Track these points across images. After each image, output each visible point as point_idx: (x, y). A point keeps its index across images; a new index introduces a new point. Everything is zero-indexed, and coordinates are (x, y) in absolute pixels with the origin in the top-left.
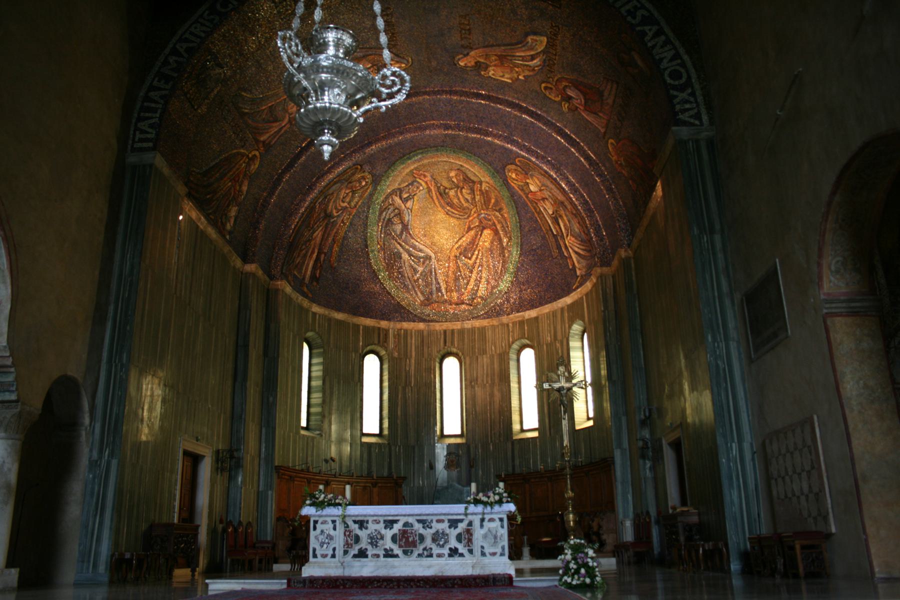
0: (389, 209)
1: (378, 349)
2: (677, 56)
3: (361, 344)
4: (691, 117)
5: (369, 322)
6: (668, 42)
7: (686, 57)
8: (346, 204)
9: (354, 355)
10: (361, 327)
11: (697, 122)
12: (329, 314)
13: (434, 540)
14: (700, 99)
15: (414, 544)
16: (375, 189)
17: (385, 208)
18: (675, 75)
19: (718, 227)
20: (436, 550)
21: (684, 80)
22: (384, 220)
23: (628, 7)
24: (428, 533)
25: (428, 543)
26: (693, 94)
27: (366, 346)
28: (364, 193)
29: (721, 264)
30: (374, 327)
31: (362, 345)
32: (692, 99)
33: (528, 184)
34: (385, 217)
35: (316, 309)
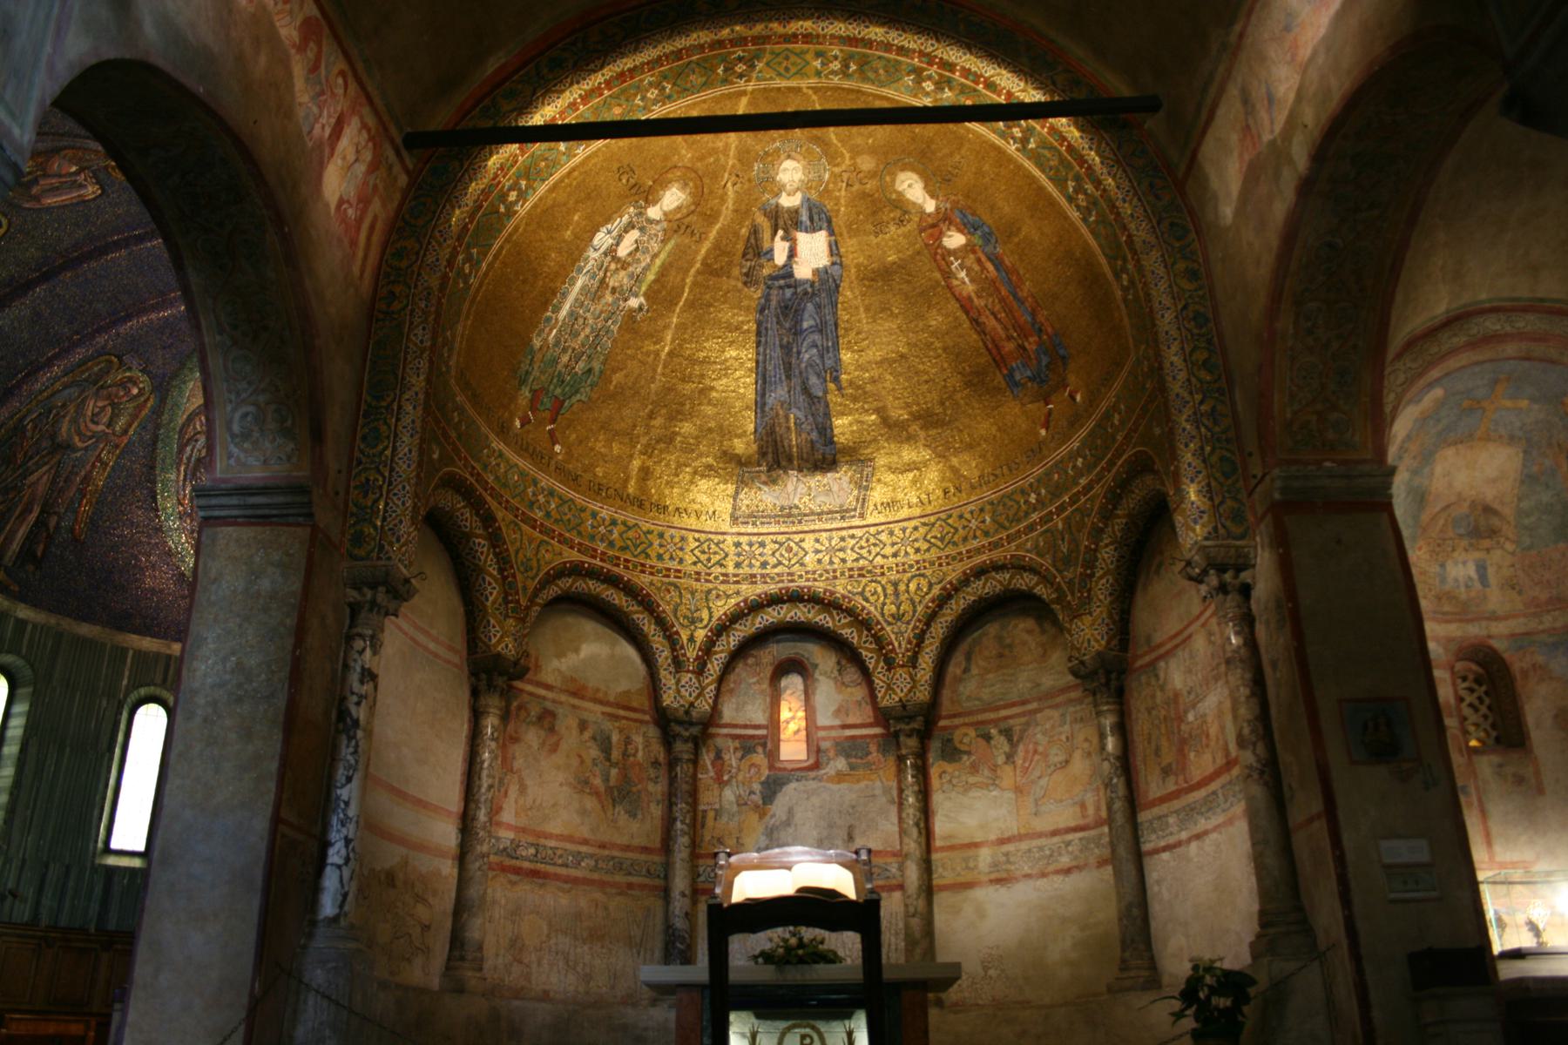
0: (197, 441)
1: (165, 694)
3: (125, 682)
5: (148, 644)
8: (101, 427)
9: (104, 703)
10: (131, 653)
12: (58, 624)
16: (163, 401)
17: (189, 440)
22: (189, 459)
27: (134, 686)
28: (140, 408)
30: (157, 655)
31: (127, 686)
34: (191, 456)
35: (24, 612)
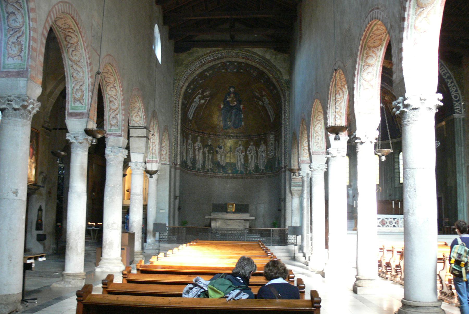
2: (456, 91)
4: (459, 111)
6: (454, 86)
7: (459, 91)
11: (460, 112)
13: (390, 223)
14: (462, 105)
15: (384, 224)
18: (456, 97)
19: (463, 144)
20: (390, 226)
21: (457, 99)
23: (444, 72)
24: (388, 221)
25: (388, 224)
26: (460, 103)
29: (463, 155)
32: (460, 105)
33: (385, 97)
